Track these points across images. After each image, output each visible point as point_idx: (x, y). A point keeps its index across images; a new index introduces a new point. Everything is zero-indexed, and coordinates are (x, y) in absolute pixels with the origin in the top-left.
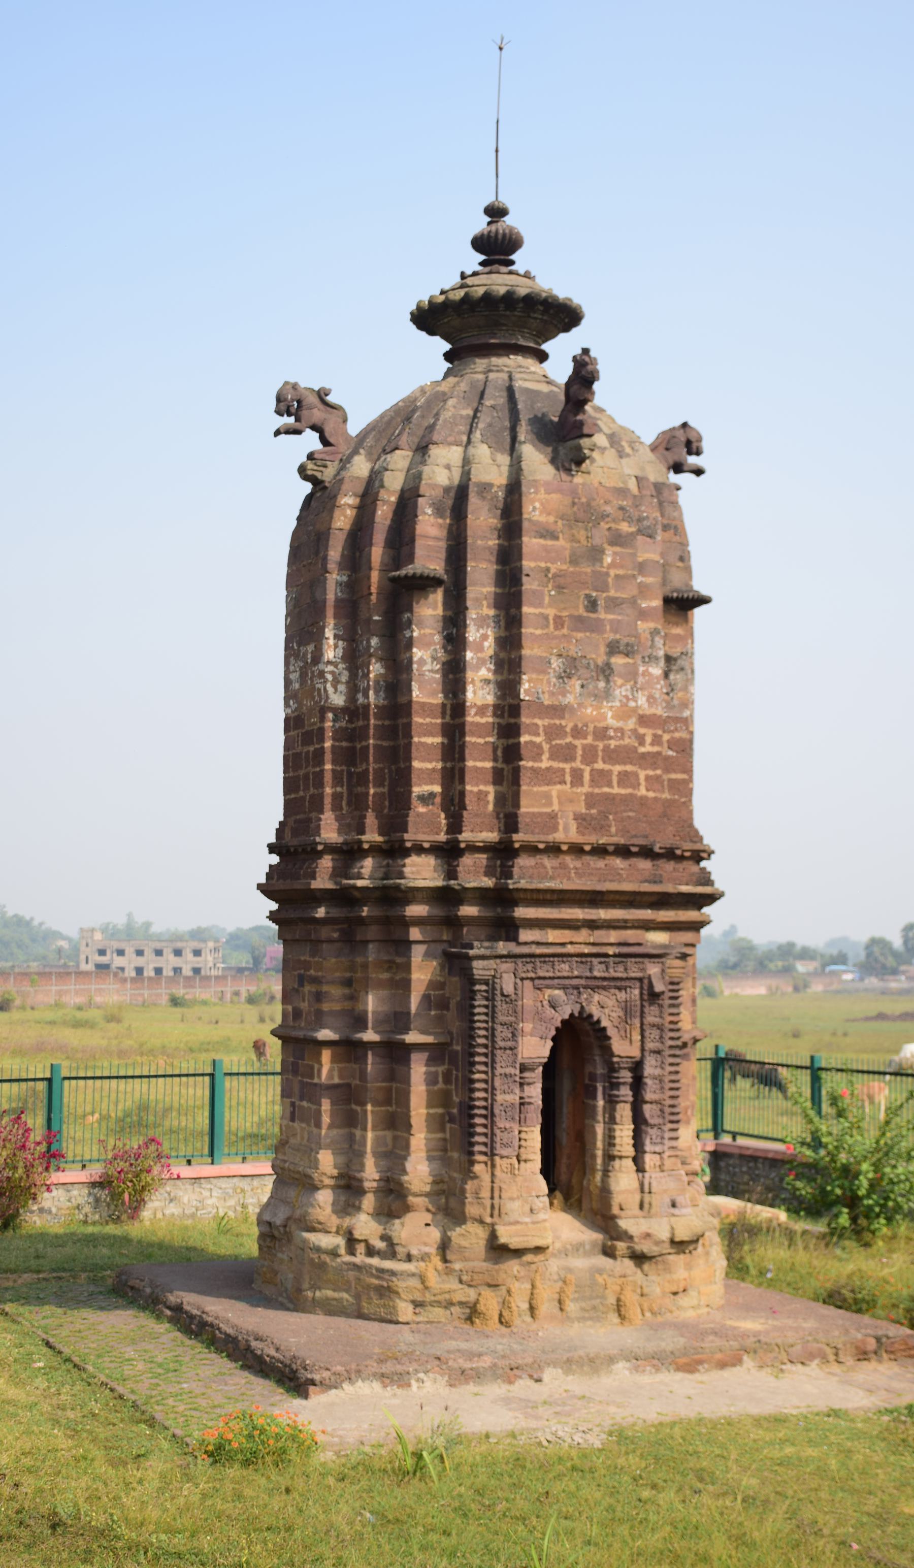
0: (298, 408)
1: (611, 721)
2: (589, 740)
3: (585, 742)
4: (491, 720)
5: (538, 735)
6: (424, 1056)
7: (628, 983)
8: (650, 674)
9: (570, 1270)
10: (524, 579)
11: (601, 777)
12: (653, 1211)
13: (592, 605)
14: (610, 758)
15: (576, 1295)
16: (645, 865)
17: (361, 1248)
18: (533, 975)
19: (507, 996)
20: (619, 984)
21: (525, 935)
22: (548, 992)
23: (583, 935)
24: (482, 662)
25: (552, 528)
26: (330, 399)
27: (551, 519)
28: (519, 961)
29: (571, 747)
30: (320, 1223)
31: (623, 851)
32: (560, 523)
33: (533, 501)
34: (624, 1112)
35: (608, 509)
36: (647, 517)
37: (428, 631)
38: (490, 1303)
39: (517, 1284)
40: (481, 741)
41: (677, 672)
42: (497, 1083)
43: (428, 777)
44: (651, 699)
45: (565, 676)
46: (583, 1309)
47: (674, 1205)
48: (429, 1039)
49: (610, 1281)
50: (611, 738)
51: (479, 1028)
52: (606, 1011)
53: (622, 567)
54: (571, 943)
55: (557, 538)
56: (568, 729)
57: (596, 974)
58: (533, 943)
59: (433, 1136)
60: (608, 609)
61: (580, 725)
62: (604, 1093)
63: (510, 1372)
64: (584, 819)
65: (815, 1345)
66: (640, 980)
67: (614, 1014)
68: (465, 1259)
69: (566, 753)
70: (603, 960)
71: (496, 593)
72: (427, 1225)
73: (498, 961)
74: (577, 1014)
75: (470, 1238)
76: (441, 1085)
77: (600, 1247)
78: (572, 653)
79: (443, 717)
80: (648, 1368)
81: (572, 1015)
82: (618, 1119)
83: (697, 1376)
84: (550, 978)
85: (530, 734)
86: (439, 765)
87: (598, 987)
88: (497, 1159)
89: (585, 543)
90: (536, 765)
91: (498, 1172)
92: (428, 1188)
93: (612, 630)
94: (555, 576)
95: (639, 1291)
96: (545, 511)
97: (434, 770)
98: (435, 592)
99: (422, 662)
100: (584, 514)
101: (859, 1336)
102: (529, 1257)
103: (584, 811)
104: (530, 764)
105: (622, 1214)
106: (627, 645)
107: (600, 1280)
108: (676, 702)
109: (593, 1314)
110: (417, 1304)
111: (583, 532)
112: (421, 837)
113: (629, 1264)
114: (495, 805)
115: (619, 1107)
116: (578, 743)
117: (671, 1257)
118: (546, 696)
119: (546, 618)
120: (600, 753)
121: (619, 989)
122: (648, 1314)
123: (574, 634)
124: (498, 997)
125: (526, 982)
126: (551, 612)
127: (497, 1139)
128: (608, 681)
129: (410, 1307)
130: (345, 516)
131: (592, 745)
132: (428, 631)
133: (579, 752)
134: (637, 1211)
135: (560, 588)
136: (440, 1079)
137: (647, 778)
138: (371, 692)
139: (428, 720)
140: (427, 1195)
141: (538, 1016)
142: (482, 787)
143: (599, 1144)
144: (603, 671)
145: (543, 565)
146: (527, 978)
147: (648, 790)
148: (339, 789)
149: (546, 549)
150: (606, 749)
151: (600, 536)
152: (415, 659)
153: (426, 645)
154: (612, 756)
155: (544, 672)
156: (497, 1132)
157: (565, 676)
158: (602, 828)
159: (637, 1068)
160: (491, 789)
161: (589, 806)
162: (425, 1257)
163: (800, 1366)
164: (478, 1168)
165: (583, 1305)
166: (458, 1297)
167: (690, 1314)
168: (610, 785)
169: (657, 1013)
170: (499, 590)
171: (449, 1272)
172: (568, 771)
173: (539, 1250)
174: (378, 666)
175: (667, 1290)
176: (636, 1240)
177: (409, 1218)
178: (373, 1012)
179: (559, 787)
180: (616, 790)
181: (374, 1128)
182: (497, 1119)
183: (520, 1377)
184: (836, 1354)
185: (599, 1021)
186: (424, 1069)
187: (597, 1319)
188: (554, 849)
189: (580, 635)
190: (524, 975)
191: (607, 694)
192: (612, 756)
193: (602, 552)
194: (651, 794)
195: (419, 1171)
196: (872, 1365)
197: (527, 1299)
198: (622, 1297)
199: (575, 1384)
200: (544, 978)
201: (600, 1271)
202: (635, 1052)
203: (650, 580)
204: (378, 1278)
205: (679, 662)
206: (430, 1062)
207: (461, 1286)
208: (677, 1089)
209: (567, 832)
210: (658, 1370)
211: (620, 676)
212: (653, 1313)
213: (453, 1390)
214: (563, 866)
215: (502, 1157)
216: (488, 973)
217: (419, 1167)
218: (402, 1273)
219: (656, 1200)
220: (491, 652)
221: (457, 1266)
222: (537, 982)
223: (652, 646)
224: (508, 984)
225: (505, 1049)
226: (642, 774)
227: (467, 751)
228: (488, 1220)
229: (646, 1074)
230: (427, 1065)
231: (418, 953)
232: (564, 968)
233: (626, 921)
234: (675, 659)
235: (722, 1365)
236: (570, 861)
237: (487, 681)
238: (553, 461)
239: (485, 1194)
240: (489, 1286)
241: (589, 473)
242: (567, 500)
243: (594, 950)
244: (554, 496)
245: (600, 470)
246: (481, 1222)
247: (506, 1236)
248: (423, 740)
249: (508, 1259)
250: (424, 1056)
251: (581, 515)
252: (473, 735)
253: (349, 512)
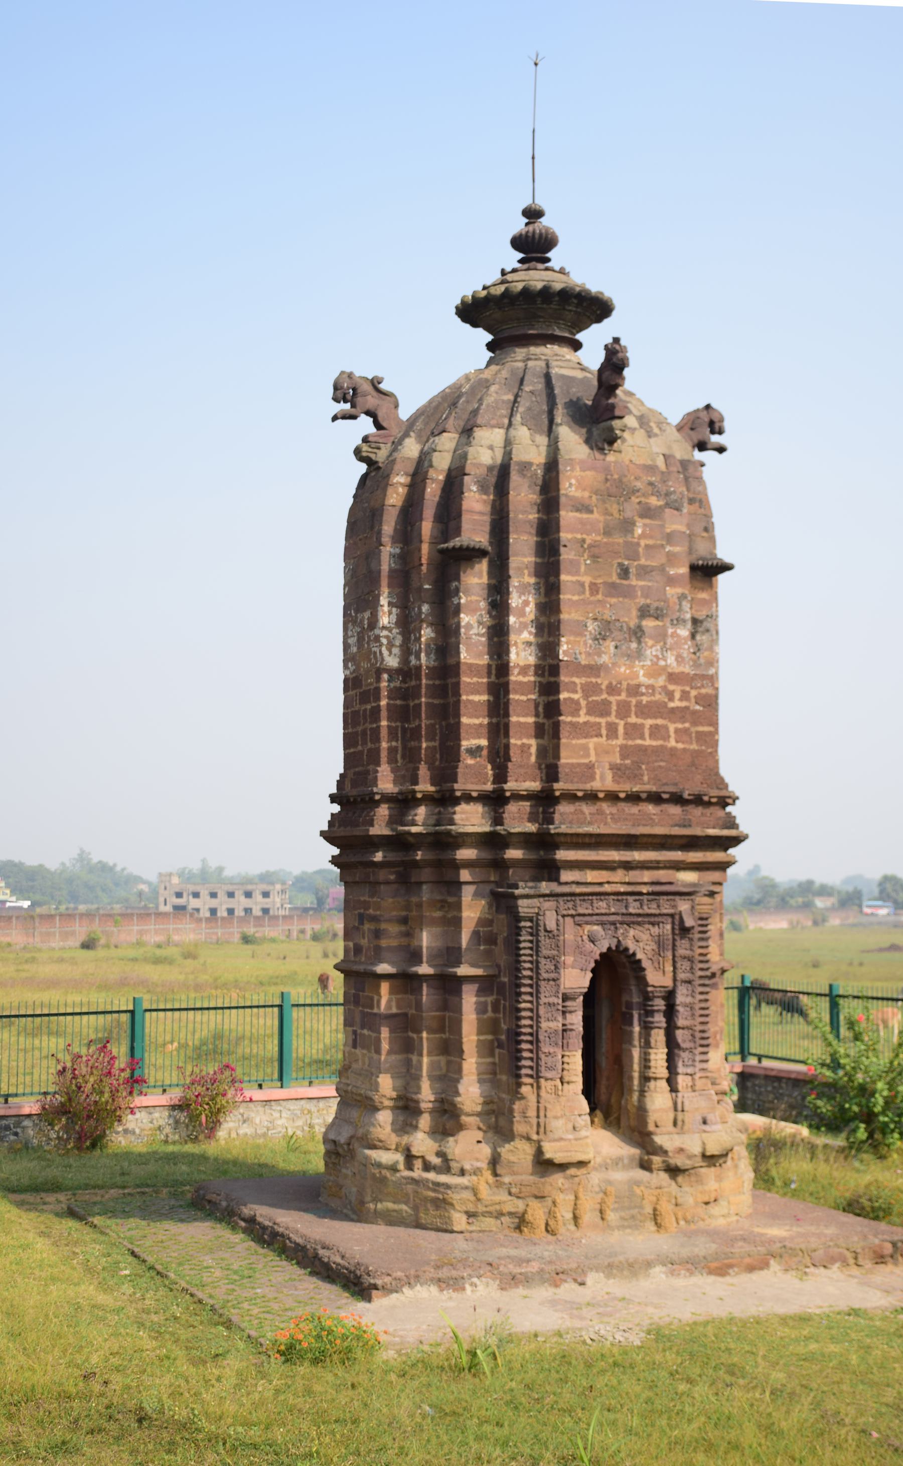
0: (354, 395)
1: (643, 679)
2: (623, 696)
3: (619, 698)
4: (532, 679)
5: (576, 692)
6: (474, 987)
7: (660, 919)
8: (678, 636)
9: (609, 1182)
10: (562, 549)
11: (634, 731)
12: (686, 1128)
13: (625, 573)
14: (643, 713)
15: (616, 1206)
16: (675, 810)
17: (418, 1164)
18: (574, 912)
19: (550, 932)
20: (652, 919)
21: (566, 876)
22: (588, 928)
23: (619, 875)
24: (524, 626)
25: (587, 502)
26: (382, 386)
27: (586, 494)
28: (561, 899)
29: (606, 703)
30: (381, 1141)
31: (655, 798)
32: (594, 497)
33: (569, 478)
34: (658, 1037)
35: (638, 484)
36: (674, 492)
37: (474, 598)
38: (537, 1213)
39: (562, 1196)
40: (524, 698)
41: (703, 633)
42: (542, 1011)
43: (476, 731)
44: (679, 659)
45: (600, 638)
46: (622, 1218)
47: (705, 1122)
48: (479, 972)
49: (647, 1192)
50: (643, 694)
51: (525, 962)
52: (641, 944)
53: (651, 537)
54: (608, 882)
55: (591, 512)
56: (603, 687)
57: (631, 910)
58: (573, 882)
59: (484, 1060)
60: (639, 576)
61: (614, 683)
62: (640, 1020)
63: (557, 1277)
64: (619, 769)
65: (836, 1250)
66: (672, 916)
67: (648, 948)
68: (514, 1173)
69: (601, 709)
71: (536, 563)
72: (479, 1142)
73: (541, 899)
75: (518, 1153)
76: (490, 1014)
77: (637, 1162)
78: (606, 617)
79: (489, 676)
80: (683, 1272)
81: (609, 949)
82: (653, 1044)
83: (728, 1279)
84: (589, 915)
85: (568, 691)
86: (486, 721)
87: (633, 923)
88: (542, 1081)
89: (617, 516)
90: (574, 720)
91: (543, 1093)
92: (479, 1108)
93: (642, 596)
94: (590, 546)
95: (673, 1201)
96: (581, 486)
97: (481, 725)
98: (480, 562)
99: (469, 626)
100: (616, 489)
101: (877, 1241)
102: (572, 1171)
103: (618, 761)
104: (569, 719)
105: (658, 1130)
106: (657, 609)
107: (638, 1191)
108: (702, 661)
109: (632, 1223)
110: (470, 1215)
111: (615, 506)
112: (469, 787)
113: (664, 1176)
114: (538, 757)
115: (654, 1032)
116: (612, 699)
117: (703, 1170)
118: (583, 656)
119: (582, 585)
120: (633, 709)
121: (653, 924)
122: (682, 1223)
123: (608, 599)
124: (542, 933)
126: (587, 580)
127: (542, 1063)
128: (639, 642)
129: (464, 1217)
130: (398, 494)
131: (625, 701)
132: (474, 598)
133: (614, 708)
134: (671, 1128)
135: (594, 557)
136: (490, 1008)
137: (677, 731)
138: (423, 655)
139: (475, 680)
140: (478, 1114)
141: (579, 950)
142: (525, 741)
143: (636, 1067)
144: (635, 633)
145: (579, 536)
147: (677, 742)
148: (394, 744)
149: (582, 522)
150: (639, 704)
151: (631, 509)
152: (463, 624)
153: (473, 611)
154: (644, 711)
155: (581, 634)
156: (542, 1056)
157: (600, 638)
158: (636, 776)
159: (670, 996)
160: (533, 742)
161: (623, 757)
162: (477, 1172)
163: (822, 1269)
164: (525, 1090)
165: (623, 1214)
166: (508, 1208)
167: (721, 1222)
168: (642, 737)
169: (688, 946)
170: (538, 560)
171: (499, 1185)
172: (603, 725)
173: (581, 1164)
174: (429, 630)
175: (700, 1200)
176: (670, 1154)
177: (462, 1136)
178: (427, 948)
179: (595, 739)
180: (648, 742)
181: (430, 1054)
182: (541, 1045)
183: (565, 1281)
184: (856, 1258)
185: (634, 954)
186: (474, 999)
187: (636, 1227)
188: (591, 797)
189: (614, 600)
190: (565, 912)
191: (639, 654)
192: (644, 711)
193: (633, 524)
194: (680, 746)
195: (471, 1092)
196: (889, 1268)
197: (571, 1209)
198: (658, 1207)
199: (616, 1287)
200: (584, 915)
201: (638, 1183)
202: (668, 982)
203: (677, 549)
204: (434, 1191)
205: (705, 624)
206: (480, 992)
207: (510, 1198)
208: (707, 1016)
209: (603, 781)
210: (692, 1274)
211: (651, 638)
212: (687, 1221)
213: (504, 1293)
214: (600, 812)
215: (547, 1079)
216: (532, 910)
217: (471, 1089)
218: (456, 1186)
219: (688, 1117)
220: (532, 617)
221: (506, 1179)
222: (577, 918)
223: (680, 610)
226: (672, 727)
227: (511, 708)
228: (535, 1137)
229: (678, 1002)
230: (477, 996)
231: (468, 892)
232: (602, 906)
233: (658, 862)
234: (701, 622)
235: (751, 1269)
236: (605, 806)
237: (529, 644)
238: (587, 441)
239: (532, 1113)
240: (536, 1197)
241: (620, 452)
242: (601, 477)
244: (588, 473)
245: (630, 449)
246: (528, 1139)
247: (551, 1151)
248: (471, 697)
249: (552, 1173)
250: (474, 987)
251: (614, 490)
252: (516, 693)
253: (400, 490)
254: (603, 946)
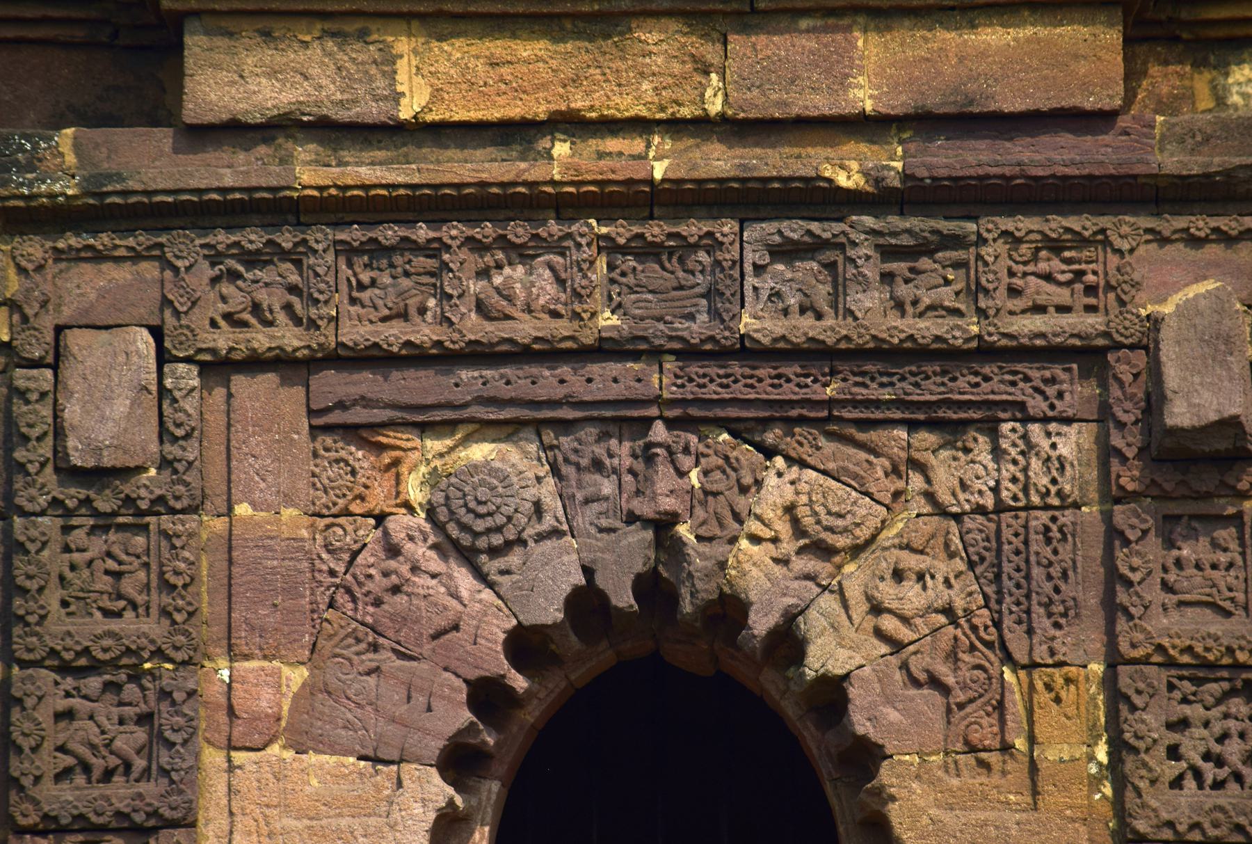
7: (996, 384)
18: (291, 338)
19: (98, 476)
20: (930, 391)
28: (187, 247)
52: (854, 575)
54: (570, 124)
66: (1089, 357)
67: (912, 596)
70: (794, 229)
74: (624, 598)
81: (586, 602)
84: (415, 357)
125: (253, 391)
146: (255, 363)
185: (788, 641)
190: (223, 340)
200: (375, 358)
222: (332, 385)
224: (106, 399)
232: (531, 296)
243: (719, 161)
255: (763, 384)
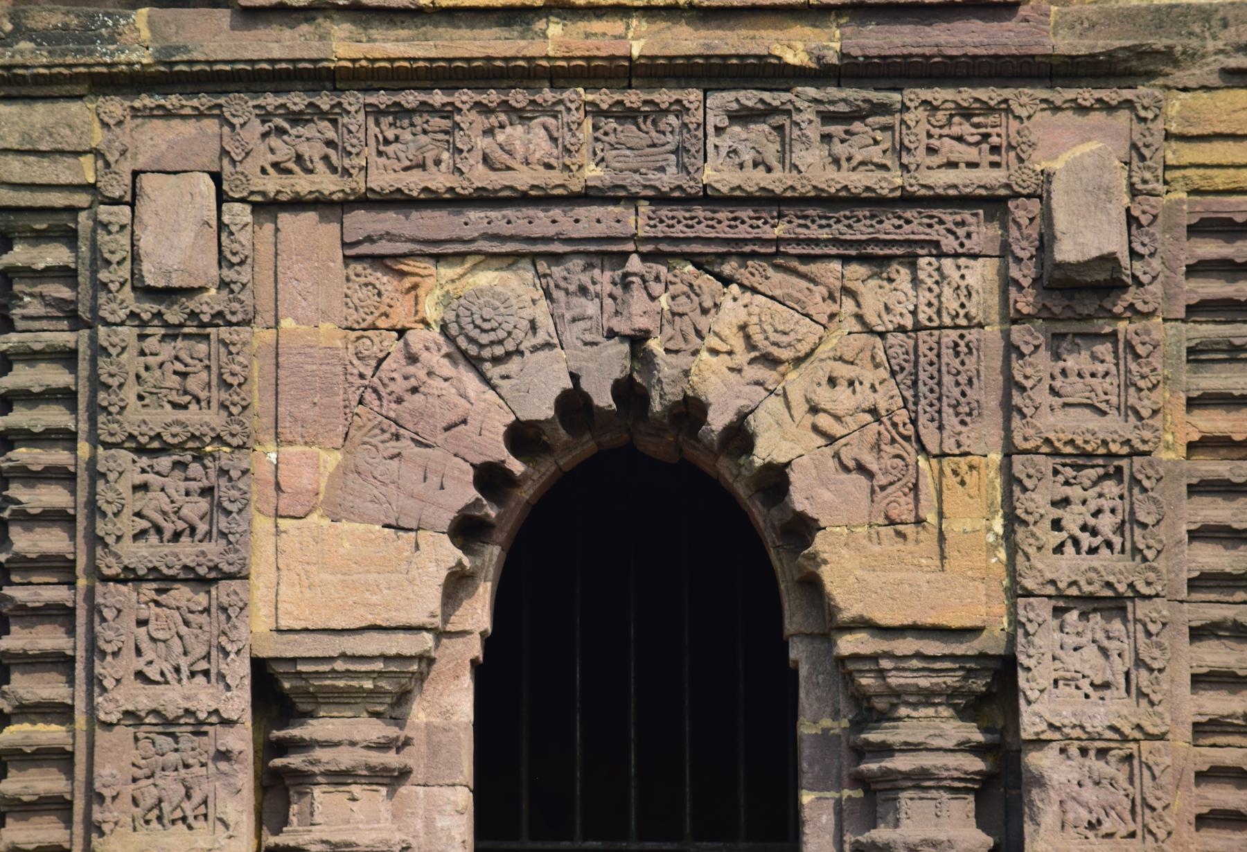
7: (916, 226)
18: (327, 184)
19: (168, 294)
22: (439, 286)
28: (240, 106)
42: (115, 761)
51: (30, 477)
52: (797, 382)
57: (717, 174)
66: (993, 204)
67: (842, 399)
70: (750, 98)
73: (115, 106)
74: (604, 399)
81: (573, 403)
84: (432, 201)
121: (876, 259)
125: (299, 227)
141: (378, 409)
146: (298, 204)
159: (992, 688)
185: (740, 436)
190: (272, 184)
202: (966, 596)
216: (61, 172)
222: (361, 222)
224: (174, 233)
225: (163, 580)
229: (1030, 724)
232: (529, 149)
254: (537, 392)
255: (723, 225)
